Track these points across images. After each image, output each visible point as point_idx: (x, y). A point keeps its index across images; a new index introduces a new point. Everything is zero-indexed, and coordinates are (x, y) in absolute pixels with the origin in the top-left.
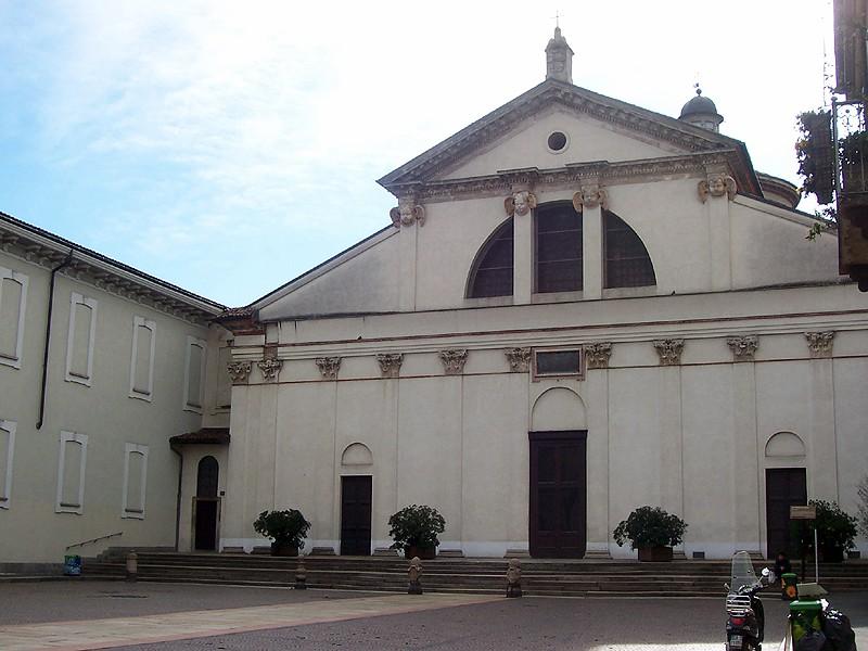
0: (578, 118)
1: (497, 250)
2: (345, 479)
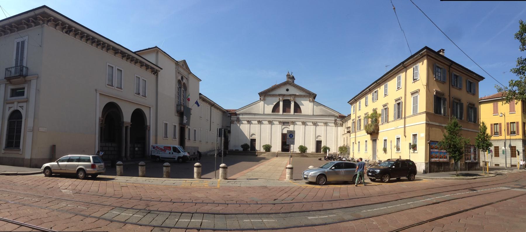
1: (277, 105)
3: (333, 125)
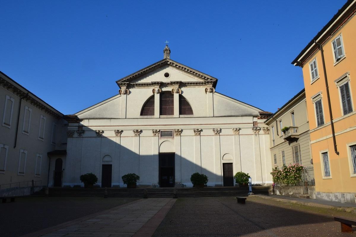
0: (172, 69)
1: (150, 102)
2: (103, 165)
3: (251, 131)
